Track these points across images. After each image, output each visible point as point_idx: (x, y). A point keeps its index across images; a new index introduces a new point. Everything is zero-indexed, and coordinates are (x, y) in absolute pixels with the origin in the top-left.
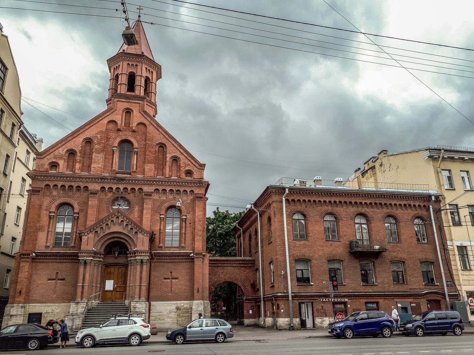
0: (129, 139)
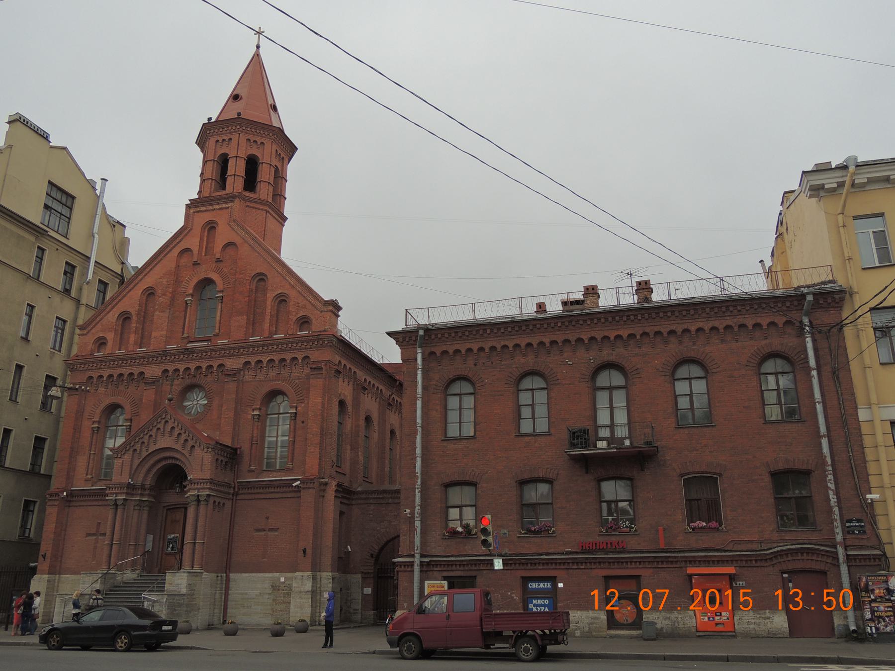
0: (209, 276)
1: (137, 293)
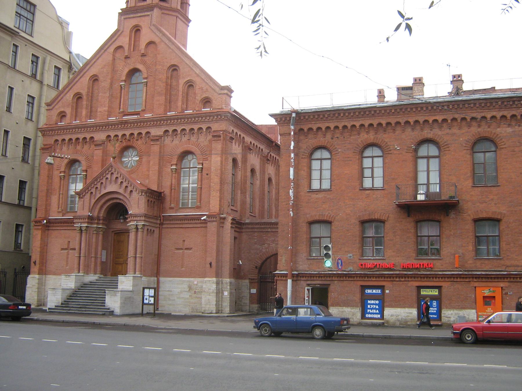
1: (85, 80)
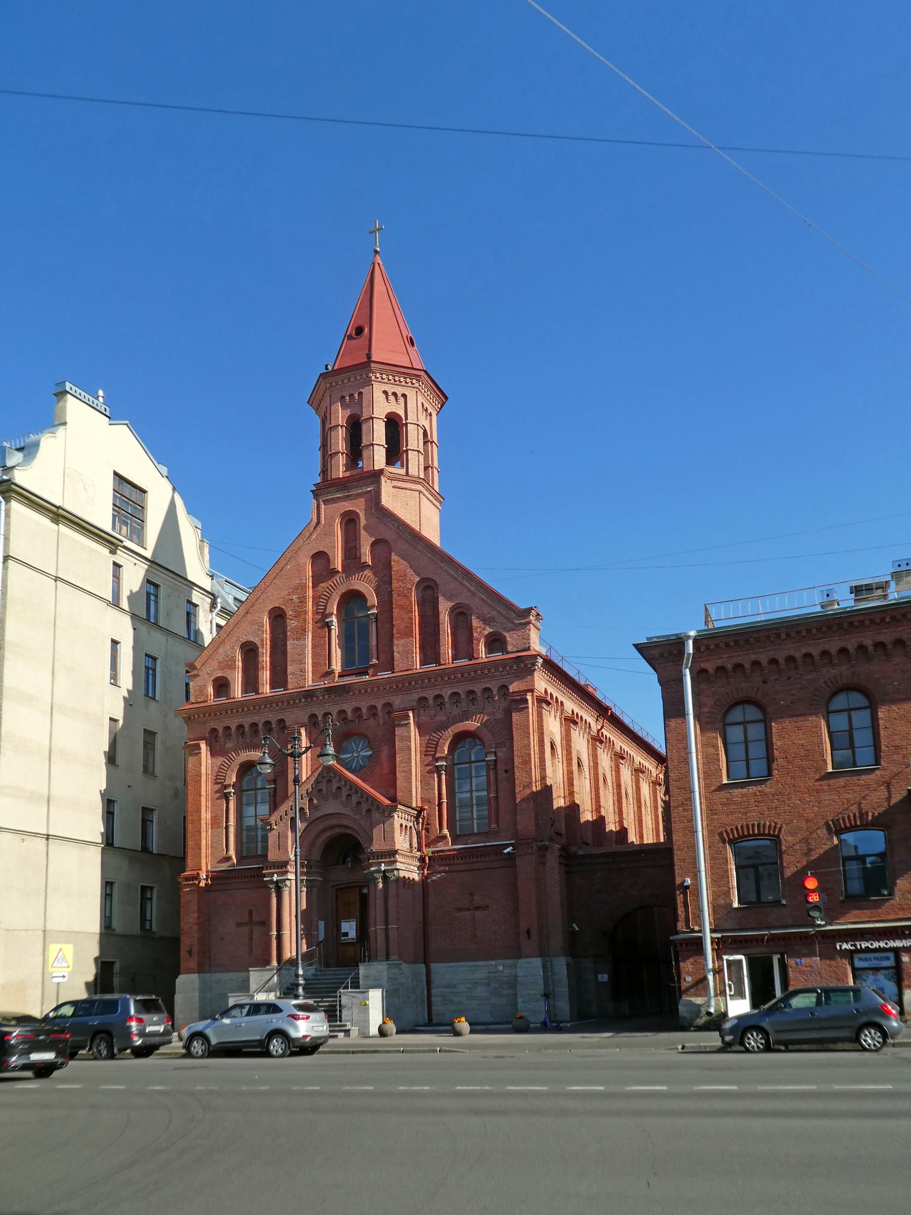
0: (356, 588)
